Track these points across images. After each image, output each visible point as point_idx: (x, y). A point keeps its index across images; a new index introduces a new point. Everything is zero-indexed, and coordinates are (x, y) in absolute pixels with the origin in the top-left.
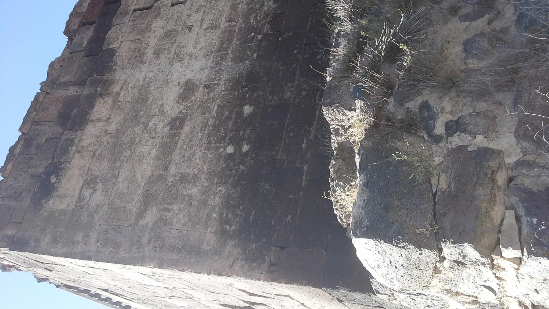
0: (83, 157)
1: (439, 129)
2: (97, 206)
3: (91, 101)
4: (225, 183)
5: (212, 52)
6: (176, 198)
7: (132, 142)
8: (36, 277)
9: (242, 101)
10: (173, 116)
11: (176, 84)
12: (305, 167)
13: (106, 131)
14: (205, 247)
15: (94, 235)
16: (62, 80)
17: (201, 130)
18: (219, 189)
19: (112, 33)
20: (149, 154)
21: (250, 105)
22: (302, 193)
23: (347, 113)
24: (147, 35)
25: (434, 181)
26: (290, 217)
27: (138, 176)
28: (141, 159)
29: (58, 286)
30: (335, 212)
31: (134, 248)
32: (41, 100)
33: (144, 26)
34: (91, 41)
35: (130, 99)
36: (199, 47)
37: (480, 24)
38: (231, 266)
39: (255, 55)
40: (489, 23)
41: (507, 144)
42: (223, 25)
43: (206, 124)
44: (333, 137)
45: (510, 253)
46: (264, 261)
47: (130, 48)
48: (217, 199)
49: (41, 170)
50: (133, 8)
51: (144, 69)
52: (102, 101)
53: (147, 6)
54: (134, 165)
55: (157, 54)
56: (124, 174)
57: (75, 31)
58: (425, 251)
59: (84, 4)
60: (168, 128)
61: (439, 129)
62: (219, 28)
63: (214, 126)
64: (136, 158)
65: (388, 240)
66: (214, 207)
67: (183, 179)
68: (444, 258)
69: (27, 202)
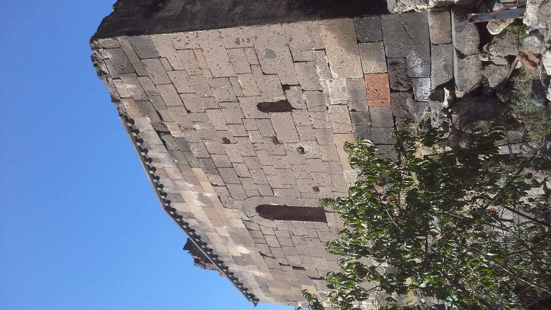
8: (112, 97)
14: (278, 14)
29: (121, 115)
46: (318, 14)
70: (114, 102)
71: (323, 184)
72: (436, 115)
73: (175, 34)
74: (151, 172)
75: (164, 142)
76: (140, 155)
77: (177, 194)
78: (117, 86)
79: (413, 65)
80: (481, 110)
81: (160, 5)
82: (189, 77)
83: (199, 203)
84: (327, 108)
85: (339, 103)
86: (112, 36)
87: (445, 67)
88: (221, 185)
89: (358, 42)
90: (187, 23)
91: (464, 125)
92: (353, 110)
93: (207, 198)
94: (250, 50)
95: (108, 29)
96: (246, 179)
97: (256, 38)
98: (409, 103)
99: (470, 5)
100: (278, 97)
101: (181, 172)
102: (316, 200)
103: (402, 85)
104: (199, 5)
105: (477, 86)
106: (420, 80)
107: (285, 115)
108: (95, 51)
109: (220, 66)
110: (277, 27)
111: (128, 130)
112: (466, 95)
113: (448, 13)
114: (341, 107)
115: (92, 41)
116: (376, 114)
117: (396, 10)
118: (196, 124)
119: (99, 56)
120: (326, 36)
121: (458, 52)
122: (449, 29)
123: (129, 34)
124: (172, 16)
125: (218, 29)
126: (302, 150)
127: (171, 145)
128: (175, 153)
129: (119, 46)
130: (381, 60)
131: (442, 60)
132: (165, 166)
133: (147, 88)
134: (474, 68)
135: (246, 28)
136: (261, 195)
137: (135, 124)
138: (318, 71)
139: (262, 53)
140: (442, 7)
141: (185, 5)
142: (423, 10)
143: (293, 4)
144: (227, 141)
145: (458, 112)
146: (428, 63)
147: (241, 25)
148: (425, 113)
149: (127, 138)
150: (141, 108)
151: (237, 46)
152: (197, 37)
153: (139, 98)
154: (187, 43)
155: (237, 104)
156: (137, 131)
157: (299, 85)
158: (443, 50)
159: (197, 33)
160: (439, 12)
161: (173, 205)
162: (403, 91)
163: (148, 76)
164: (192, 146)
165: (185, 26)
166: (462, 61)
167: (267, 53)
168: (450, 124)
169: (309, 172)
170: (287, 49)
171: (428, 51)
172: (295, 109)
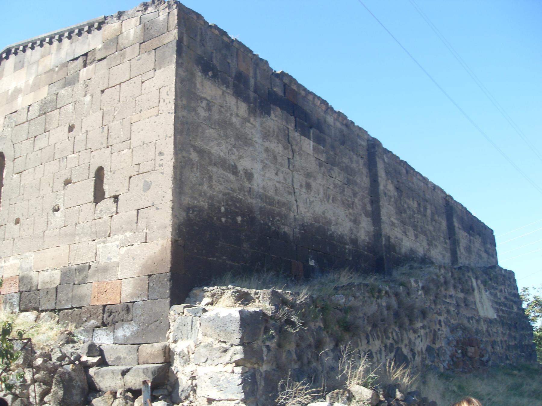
0: (220, 98)
1: (268, 343)
2: (198, 114)
3: (246, 100)
4: (209, 208)
5: (265, 191)
6: (202, 174)
7: (227, 137)
8: (124, 12)
9: (243, 215)
10: (238, 166)
11: (252, 167)
12: (215, 259)
13: (231, 114)
14: (183, 197)
15: (185, 113)
16: (258, 71)
17: (232, 188)
18: (206, 204)
19: (279, 111)
20: (221, 150)
21: (241, 221)
22: (205, 257)
23: (268, 302)
24: (276, 141)
25: (255, 342)
26: (196, 251)
27: (212, 144)
28: (219, 144)
29: (105, 18)
30: (216, 287)
31: (180, 146)
32: (250, 55)
33: (280, 138)
34: (275, 93)
35: (247, 131)
36: (268, 181)
37: (294, 356)
38: (176, 216)
39: (262, 222)
40: (294, 360)
41: (264, 368)
42: (277, 198)
43: (233, 191)
44: (254, 291)
45: (239, 370)
46: (179, 237)
47: (270, 127)
48: (202, 203)
49: (215, 62)
50: (290, 127)
51: (260, 141)
52: (246, 109)
53: (290, 139)
54: (216, 139)
55: (267, 150)
56: (212, 131)
57: (282, 80)
58: (239, 340)
59: (295, 86)
60: (233, 164)
61: (268, 343)
62: (276, 195)
63: (233, 197)
64: (219, 141)
65: (241, 326)
66: (199, 202)
67: (210, 178)
68: (232, 346)
69: (199, 52)
70: (119, 14)
71: (22, 229)
72: (77, 349)
73: (173, 90)
74: (48, 40)
75: (76, 59)
76: (66, 31)
77: (23, 64)
78: (134, 19)
79: (125, 328)
80: (74, 391)
81: (210, 74)
82: (134, 97)
83: (12, 88)
84: (94, 240)
85: (98, 253)
86: (179, 24)
87: (118, 358)
88: (29, 116)
89: (150, 276)
90: (184, 102)
91: (60, 377)
92: (90, 267)
93: (16, 98)
94: (153, 165)
95: (188, 20)
96: (32, 145)
97: (162, 173)
98: (93, 322)
99: (168, 380)
100: (109, 189)
101: (45, 73)
102: (6, 220)
103: (109, 316)
104: (205, 115)
105: (98, 387)
106: (112, 334)
107: (90, 196)
108: (166, 4)
109: (141, 132)
110: (169, 196)
111: (91, 23)
112: (89, 378)
113: (162, 361)
114: (93, 254)
115: (176, 2)
116: (84, 289)
117: (172, 313)
118: (90, 97)
119: (162, 7)
120: (157, 244)
121: (128, 370)
122: (150, 361)
123: (179, 43)
124: (195, 86)
125: (175, 135)
126: (56, 210)
127: (72, 66)
128: (65, 69)
129: (169, 29)
130: (132, 297)
131: (125, 355)
132: (53, 55)
133: (128, 50)
134: (113, 385)
135: (171, 164)
136: (15, 159)
137: (96, 30)
138: (128, 234)
139: (149, 178)
140: (170, 356)
141: (207, 100)
142: (168, 338)
143: (193, 211)
144: (71, 129)
145: (73, 370)
146: (125, 342)
147: (176, 160)
148: (82, 338)
149: (83, 21)
150: (111, 41)
151: (157, 152)
152: (169, 113)
153: (120, 41)
154: (164, 101)
155: (105, 145)
156: (89, 32)
157: (117, 213)
158: (134, 356)
159: (172, 113)
160: (165, 353)
161: (12, 57)
162: (103, 317)
163: (139, 54)
164: (69, 89)
165: (182, 101)
166: (120, 373)
167: (148, 182)
168: (63, 363)
169: (35, 215)
170: (150, 204)
171: (136, 342)
172: (96, 205)
